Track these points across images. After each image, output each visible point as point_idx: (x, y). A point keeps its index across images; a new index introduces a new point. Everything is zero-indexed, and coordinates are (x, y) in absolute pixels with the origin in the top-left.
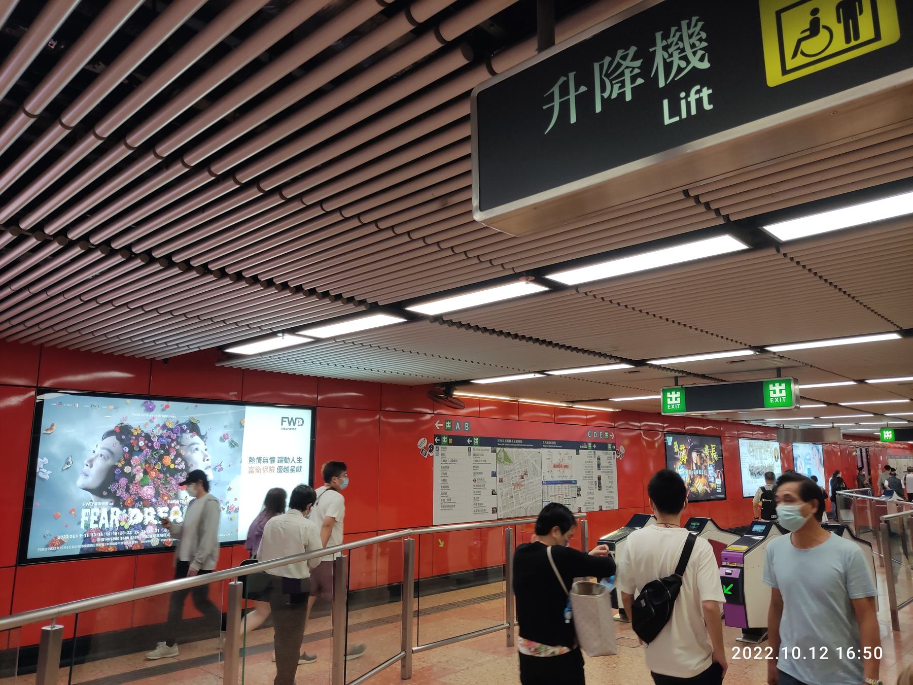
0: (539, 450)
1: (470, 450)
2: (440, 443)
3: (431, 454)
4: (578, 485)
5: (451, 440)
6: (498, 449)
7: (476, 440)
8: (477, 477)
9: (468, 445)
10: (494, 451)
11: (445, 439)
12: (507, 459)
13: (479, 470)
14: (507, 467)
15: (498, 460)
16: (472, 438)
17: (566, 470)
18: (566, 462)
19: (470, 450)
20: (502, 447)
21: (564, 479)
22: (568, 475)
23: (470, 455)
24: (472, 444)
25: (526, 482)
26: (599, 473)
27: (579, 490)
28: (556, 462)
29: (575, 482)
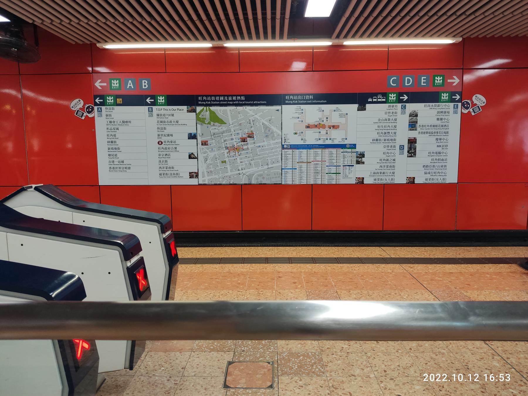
0: (279, 107)
1: (151, 111)
2: (103, 104)
3: (90, 116)
4: (359, 149)
5: (119, 101)
6: (199, 109)
7: (161, 99)
8: (163, 139)
9: (147, 104)
10: (195, 111)
11: (110, 100)
12: (215, 119)
13: (166, 132)
14: (216, 129)
15: (200, 120)
16: (153, 97)
17: (333, 132)
18: (335, 119)
19: (151, 111)
20: (206, 105)
21: (329, 142)
22: (337, 137)
23: (151, 115)
24: (154, 104)
25: (250, 146)
26: (413, 134)
27: (362, 155)
28: (312, 121)
29: (354, 146)
